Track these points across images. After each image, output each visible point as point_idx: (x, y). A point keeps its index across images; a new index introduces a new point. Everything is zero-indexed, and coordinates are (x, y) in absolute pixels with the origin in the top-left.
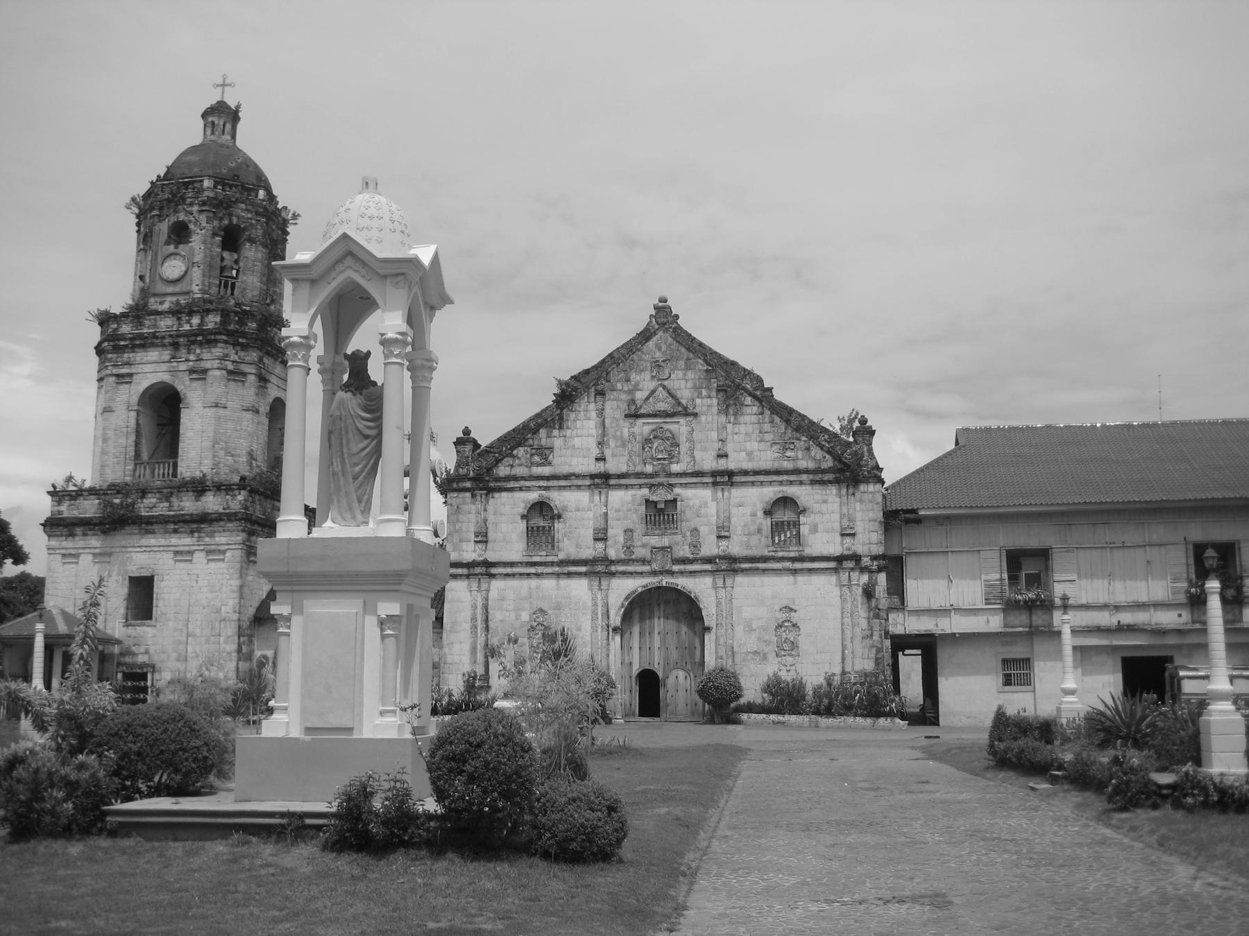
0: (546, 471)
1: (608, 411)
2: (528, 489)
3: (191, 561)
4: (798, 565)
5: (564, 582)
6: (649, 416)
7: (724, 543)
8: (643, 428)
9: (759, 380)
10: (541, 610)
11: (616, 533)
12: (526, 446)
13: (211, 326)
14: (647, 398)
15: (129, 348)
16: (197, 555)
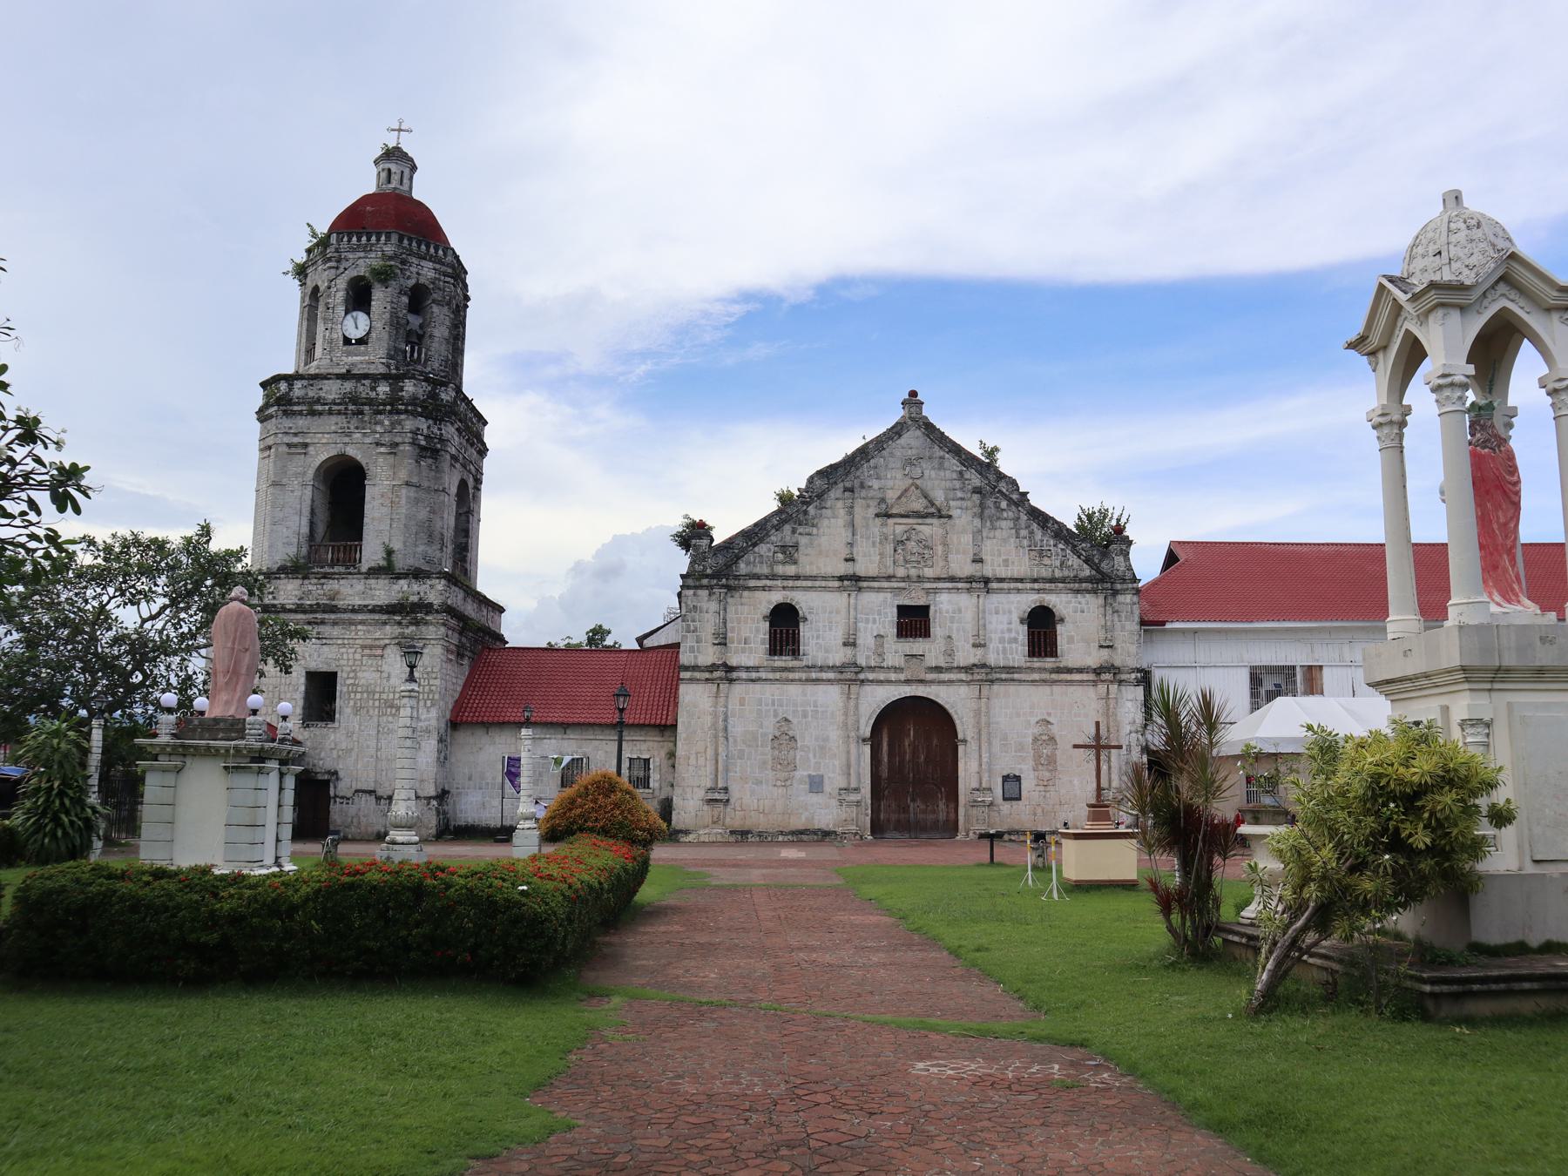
0: (791, 570)
1: (858, 510)
2: (770, 589)
3: (382, 656)
4: (1054, 676)
5: (810, 688)
6: (902, 516)
7: (980, 651)
8: (897, 527)
9: (1014, 483)
10: (786, 720)
11: (866, 639)
12: (768, 543)
14: (899, 498)
16: (388, 651)
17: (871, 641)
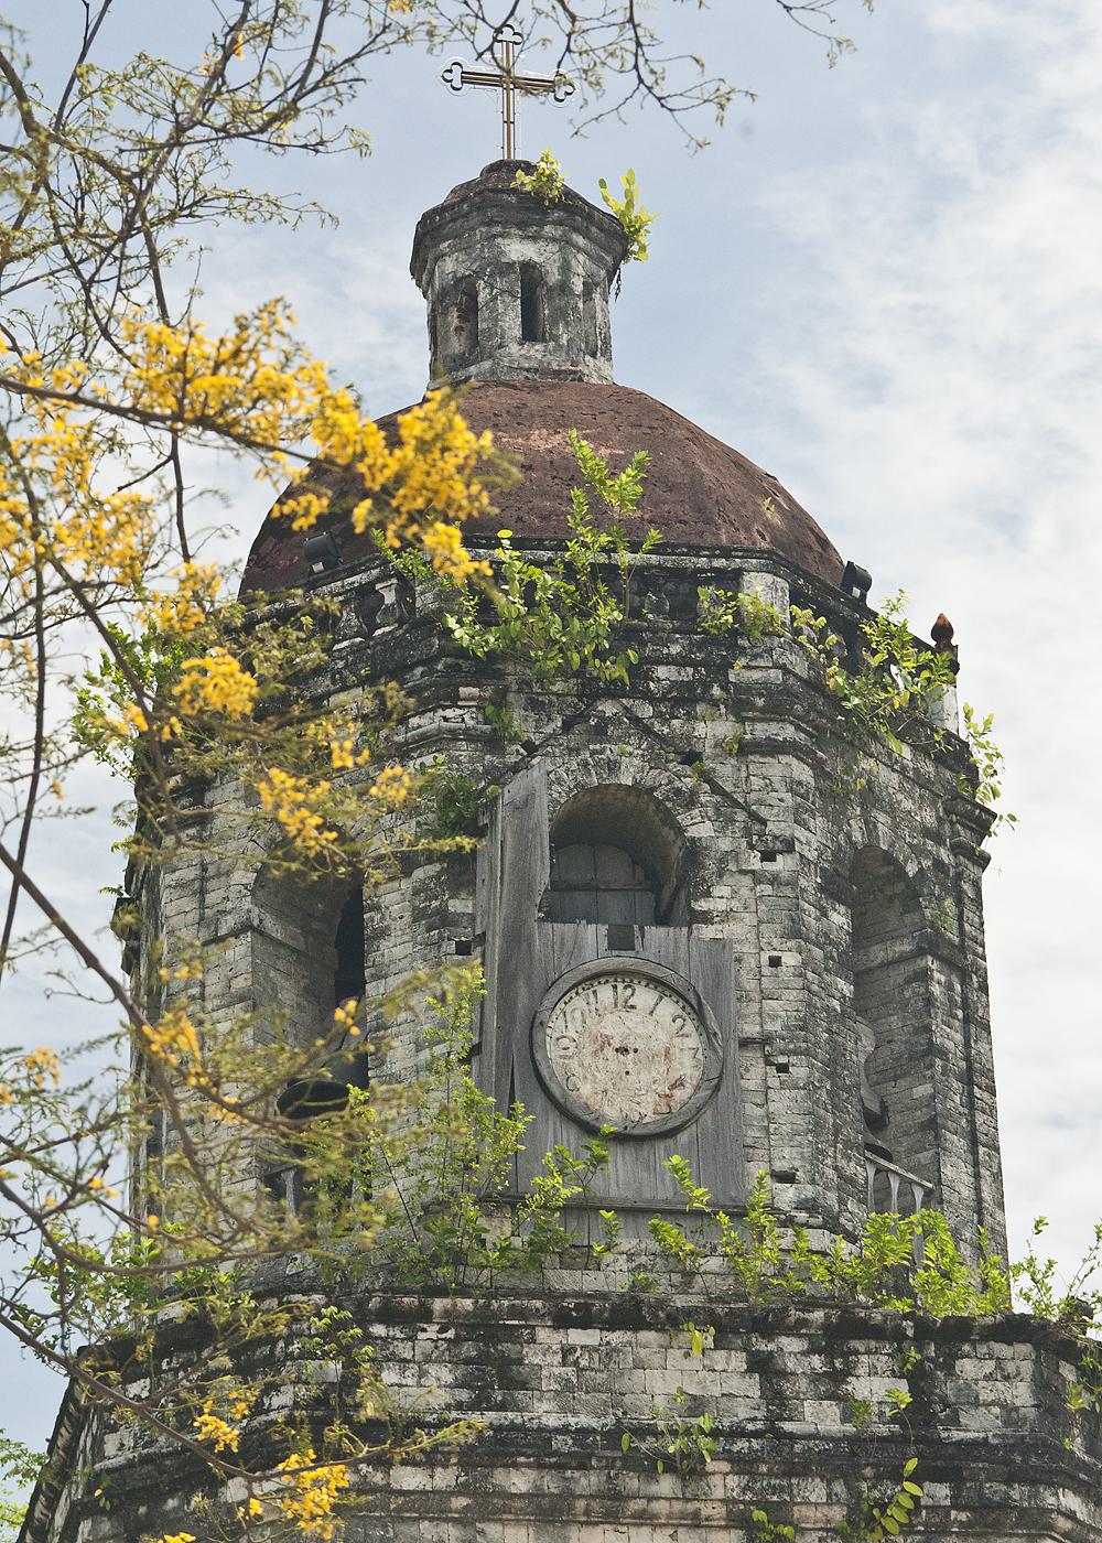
13: (978, 1425)
15: (441, 1515)
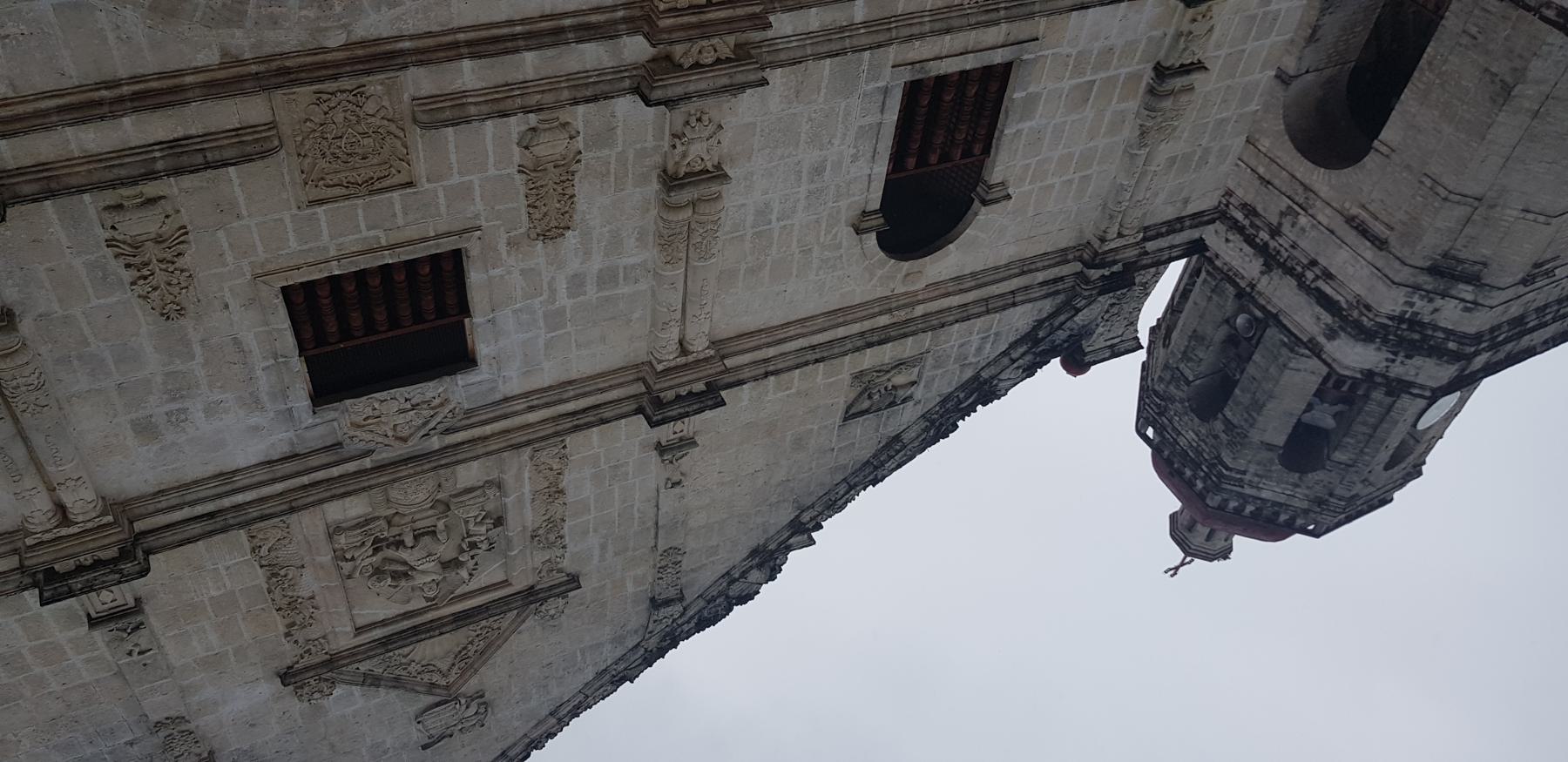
17: (591, 200)
